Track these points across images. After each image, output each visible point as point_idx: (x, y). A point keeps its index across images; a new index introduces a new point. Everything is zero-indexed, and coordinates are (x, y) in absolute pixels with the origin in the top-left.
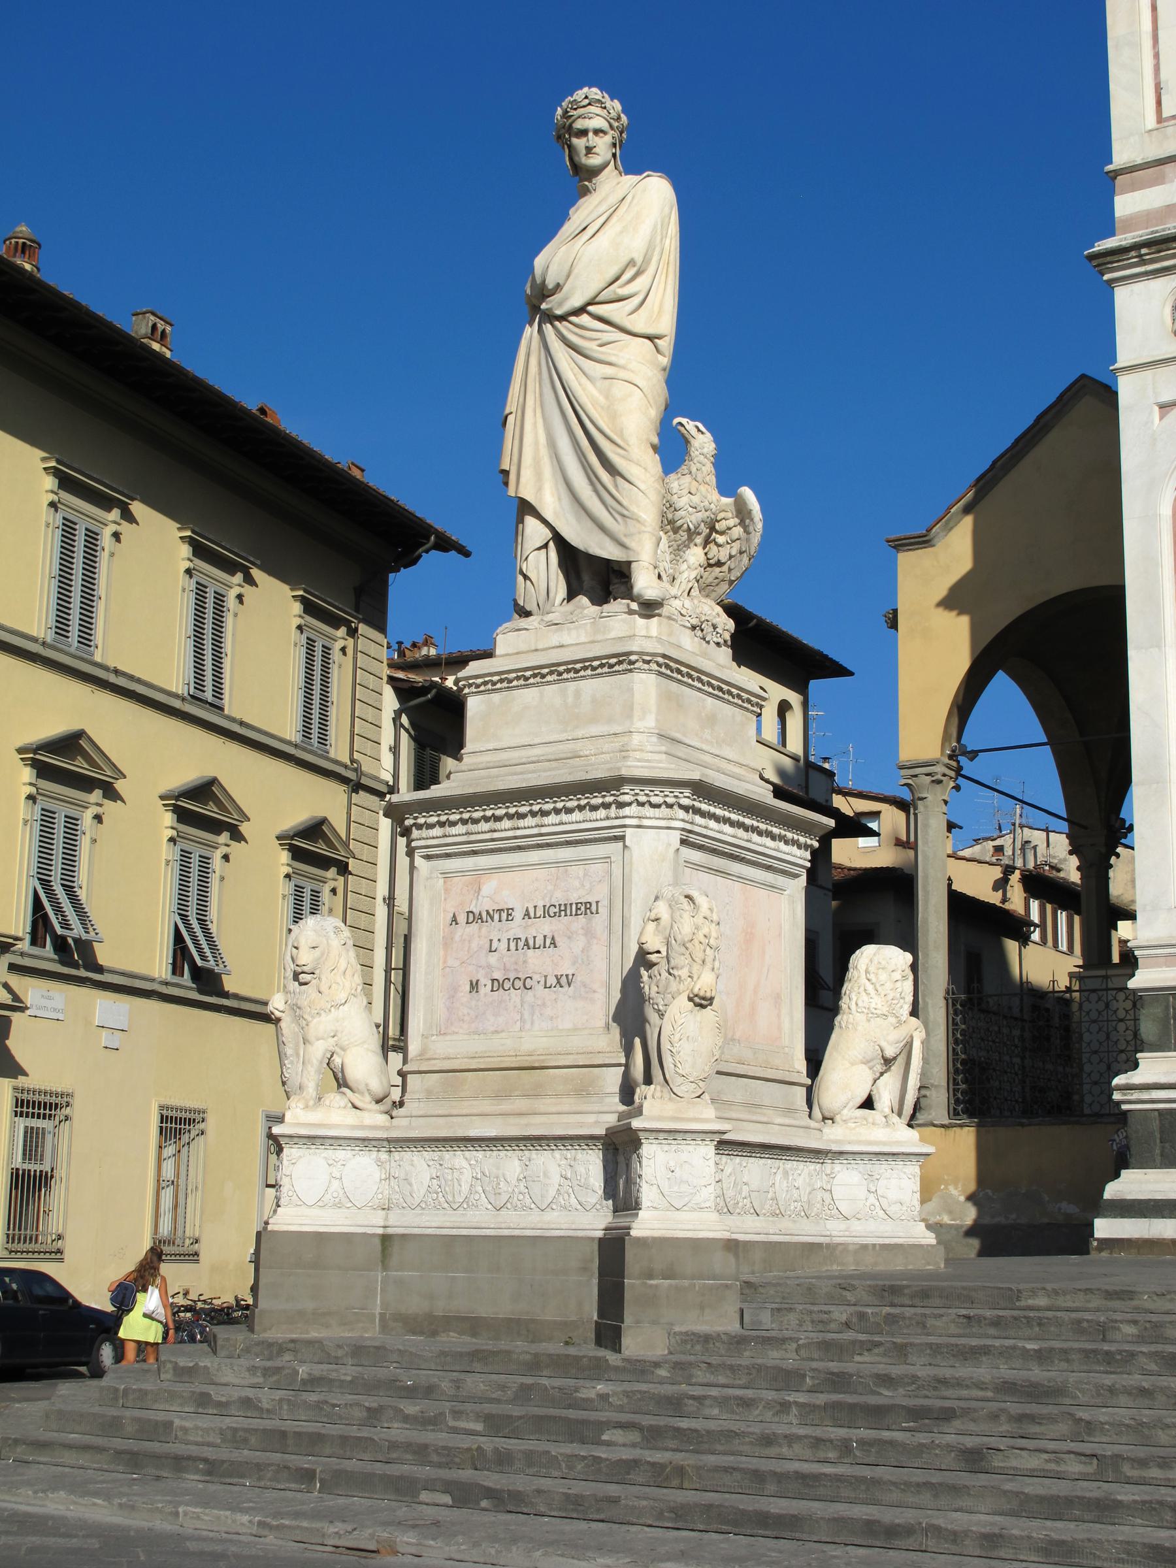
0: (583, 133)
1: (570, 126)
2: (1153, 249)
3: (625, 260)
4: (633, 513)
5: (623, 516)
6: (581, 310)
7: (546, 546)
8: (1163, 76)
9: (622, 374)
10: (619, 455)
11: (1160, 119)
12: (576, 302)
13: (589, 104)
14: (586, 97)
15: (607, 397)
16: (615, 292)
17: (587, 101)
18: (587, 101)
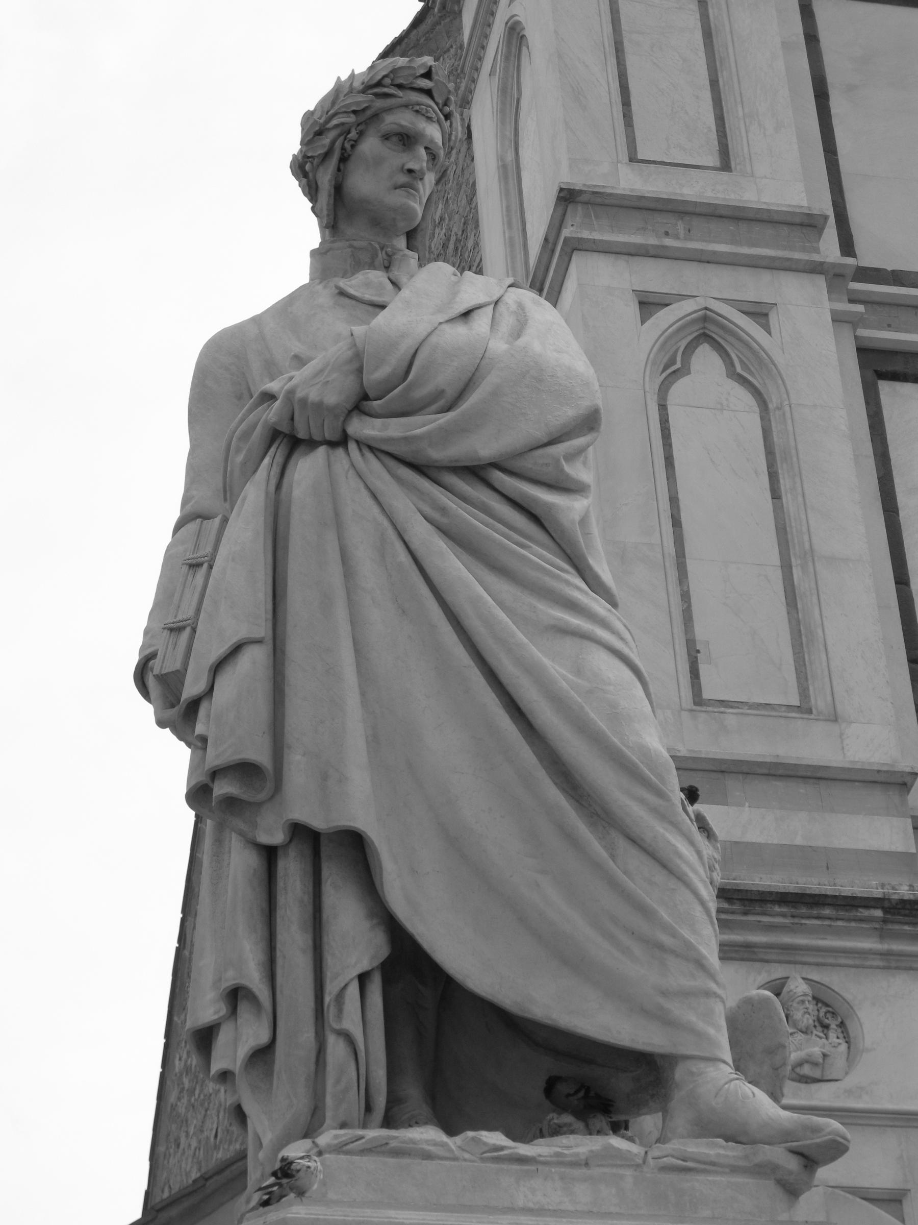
0: (406, 140)
1: (376, 116)
2: (736, 907)
3: (584, 405)
4: (688, 945)
5: (661, 947)
6: (476, 472)
7: (363, 979)
8: (700, 631)
9: (601, 633)
10: (642, 801)
11: (698, 700)
12: (484, 446)
13: (428, 93)
14: (428, 75)
15: (578, 671)
16: (558, 461)
17: (425, 83)
18: (425, 83)
